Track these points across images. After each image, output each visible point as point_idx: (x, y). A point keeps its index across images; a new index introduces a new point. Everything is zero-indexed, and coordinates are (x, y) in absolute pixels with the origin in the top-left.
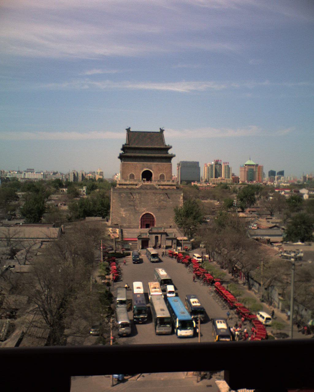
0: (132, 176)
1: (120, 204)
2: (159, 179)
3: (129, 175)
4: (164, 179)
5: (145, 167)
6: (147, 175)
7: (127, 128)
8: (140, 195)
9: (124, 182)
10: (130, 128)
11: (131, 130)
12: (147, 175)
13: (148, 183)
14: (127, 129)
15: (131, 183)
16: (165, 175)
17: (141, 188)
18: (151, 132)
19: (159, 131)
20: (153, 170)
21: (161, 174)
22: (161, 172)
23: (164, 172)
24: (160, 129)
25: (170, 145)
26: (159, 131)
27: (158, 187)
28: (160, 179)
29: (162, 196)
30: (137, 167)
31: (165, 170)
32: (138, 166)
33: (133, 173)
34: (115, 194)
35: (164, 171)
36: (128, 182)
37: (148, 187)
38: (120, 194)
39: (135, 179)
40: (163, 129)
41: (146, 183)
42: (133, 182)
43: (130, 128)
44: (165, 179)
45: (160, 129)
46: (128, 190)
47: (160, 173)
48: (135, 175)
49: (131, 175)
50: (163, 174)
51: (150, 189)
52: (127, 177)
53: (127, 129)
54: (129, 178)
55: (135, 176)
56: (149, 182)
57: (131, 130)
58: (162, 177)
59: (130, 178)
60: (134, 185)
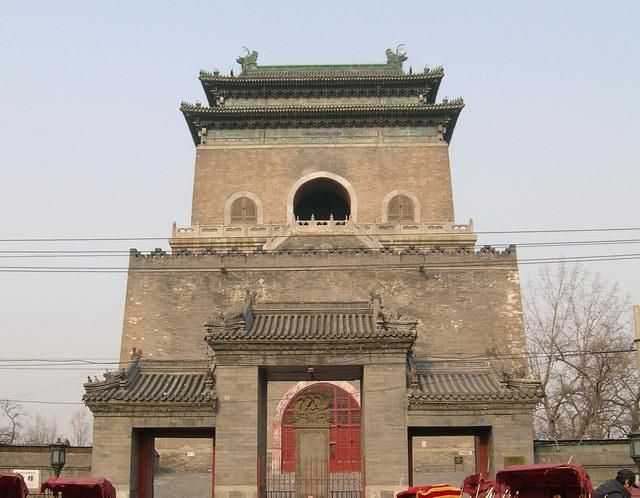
0: (244, 211)
1: (167, 337)
2: (384, 219)
3: (229, 203)
4: (411, 218)
5: (310, 164)
6: (322, 200)
7: (244, 55)
8: (275, 285)
9: (197, 234)
10: (255, 54)
11: (260, 62)
12: (322, 200)
13: (330, 227)
14: (241, 61)
15: (233, 234)
16: (415, 199)
17: (285, 250)
18: (350, 66)
19: (384, 60)
20: (349, 179)
21: (395, 193)
22: (396, 187)
23: (408, 187)
24: (388, 52)
25: (433, 68)
26: (384, 60)
27: (374, 245)
28: (390, 218)
29: (399, 290)
30: (268, 168)
31: (416, 177)
32: (276, 159)
33: (250, 195)
34: (144, 282)
35: (411, 180)
36: (220, 234)
37: (325, 246)
38: (168, 283)
39: (260, 220)
40: (402, 52)
41: (313, 227)
42: (246, 232)
43: (255, 54)
44: (417, 219)
45: (388, 52)
46: (208, 259)
47: (387, 190)
48: (258, 202)
49: (238, 202)
50: (406, 193)
51: (336, 251)
52: (222, 214)
53: (241, 61)
54: (228, 219)
55: (260, 211)
56: (331, 222)
57: (260, 62)
58: (400, 209)
59: (233, 220)
60: (250, 244)
